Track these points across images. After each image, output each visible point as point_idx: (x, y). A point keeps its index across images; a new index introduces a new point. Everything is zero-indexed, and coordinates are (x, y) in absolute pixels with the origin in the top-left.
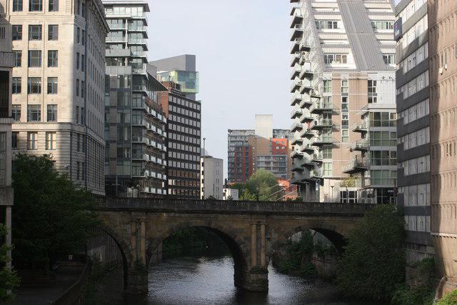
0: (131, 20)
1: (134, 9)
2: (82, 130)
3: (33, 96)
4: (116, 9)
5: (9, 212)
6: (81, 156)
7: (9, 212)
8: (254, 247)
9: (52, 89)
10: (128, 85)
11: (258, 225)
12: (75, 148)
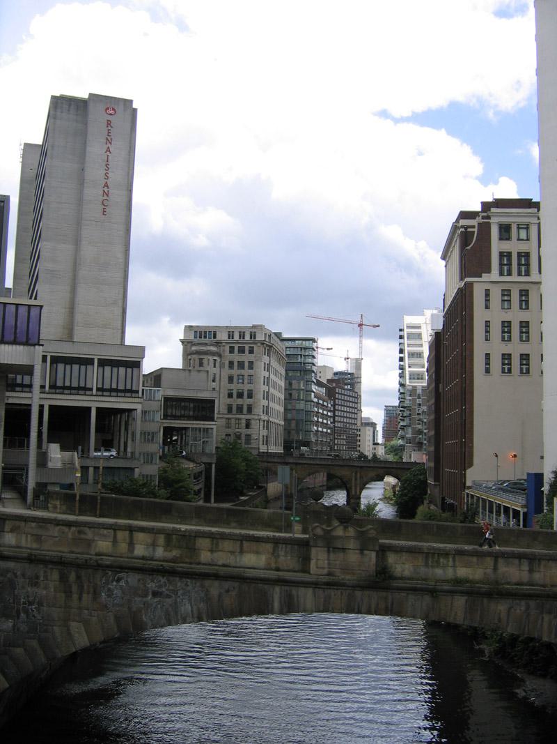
0: (305, 349)
1: (307, 342)
2: (266, 418)
3: (240, 400)
4: (297, 342)
5: (214, 466)
6: (265, 432)
7: (214, 466)
8: (353, 485)
9: (250, 396)
10: (304, 386)
11: (356, 474)
12: (261, 427)
